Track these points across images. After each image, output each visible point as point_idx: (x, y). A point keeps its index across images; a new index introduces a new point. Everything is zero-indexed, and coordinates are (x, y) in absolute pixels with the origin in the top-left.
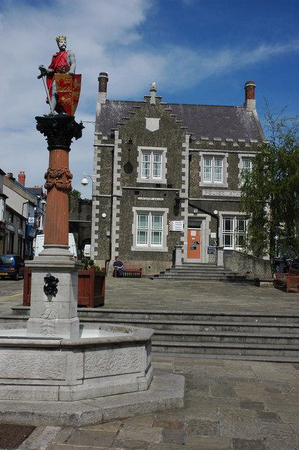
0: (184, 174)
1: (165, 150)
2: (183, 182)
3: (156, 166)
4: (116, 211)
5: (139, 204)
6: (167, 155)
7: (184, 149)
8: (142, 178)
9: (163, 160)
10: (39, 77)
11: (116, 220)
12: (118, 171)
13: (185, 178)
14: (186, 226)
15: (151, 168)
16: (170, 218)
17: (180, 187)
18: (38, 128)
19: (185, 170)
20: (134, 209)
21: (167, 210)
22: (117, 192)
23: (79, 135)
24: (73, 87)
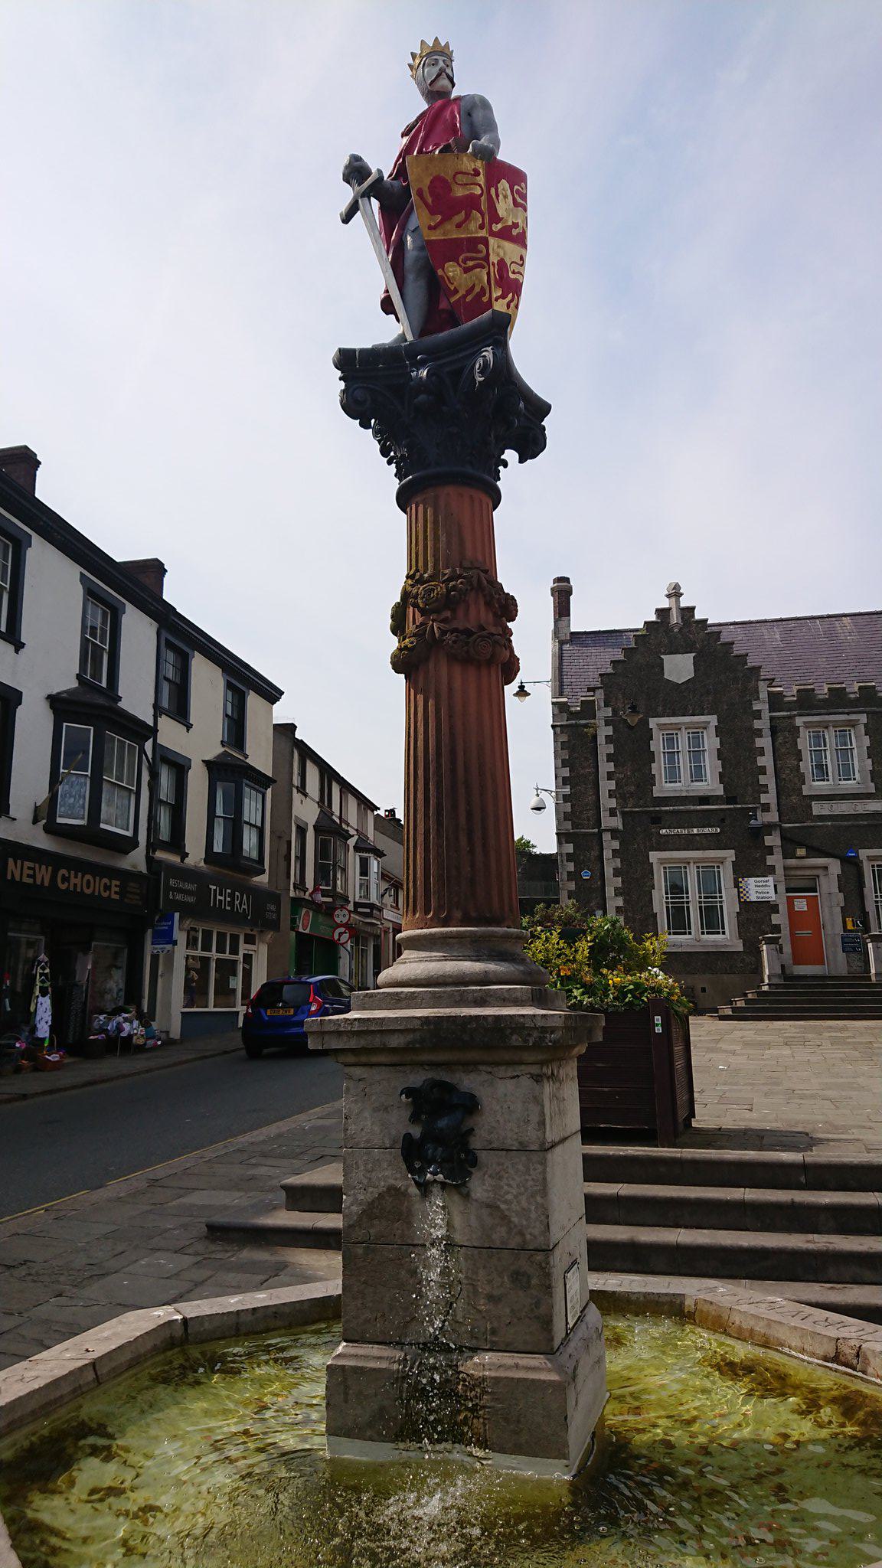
0: (763, 770)
1: (713, 720)
2: (764, 789)
3: (697, 755)
4: (610, 866)
5: (664, 845)
6: (719, 732)
7: (758, 715)
8: (663, 788)
9: (711, 742)
10: (347, 218)
11: (612, 883)
12: (610, 776)
13: (768, 780)
14: (782, 888)
15: (684, 762)
16: (743, 870)
17: (757, 800)
18: (353, 406)
19: (766, 761)
20: (654, 856)
21: (730, 855)
22: (610, 822)
23: (531, 445)
24: (495, 218)
